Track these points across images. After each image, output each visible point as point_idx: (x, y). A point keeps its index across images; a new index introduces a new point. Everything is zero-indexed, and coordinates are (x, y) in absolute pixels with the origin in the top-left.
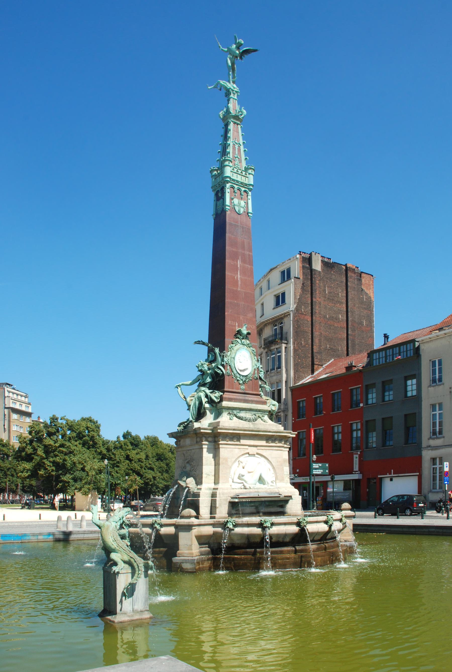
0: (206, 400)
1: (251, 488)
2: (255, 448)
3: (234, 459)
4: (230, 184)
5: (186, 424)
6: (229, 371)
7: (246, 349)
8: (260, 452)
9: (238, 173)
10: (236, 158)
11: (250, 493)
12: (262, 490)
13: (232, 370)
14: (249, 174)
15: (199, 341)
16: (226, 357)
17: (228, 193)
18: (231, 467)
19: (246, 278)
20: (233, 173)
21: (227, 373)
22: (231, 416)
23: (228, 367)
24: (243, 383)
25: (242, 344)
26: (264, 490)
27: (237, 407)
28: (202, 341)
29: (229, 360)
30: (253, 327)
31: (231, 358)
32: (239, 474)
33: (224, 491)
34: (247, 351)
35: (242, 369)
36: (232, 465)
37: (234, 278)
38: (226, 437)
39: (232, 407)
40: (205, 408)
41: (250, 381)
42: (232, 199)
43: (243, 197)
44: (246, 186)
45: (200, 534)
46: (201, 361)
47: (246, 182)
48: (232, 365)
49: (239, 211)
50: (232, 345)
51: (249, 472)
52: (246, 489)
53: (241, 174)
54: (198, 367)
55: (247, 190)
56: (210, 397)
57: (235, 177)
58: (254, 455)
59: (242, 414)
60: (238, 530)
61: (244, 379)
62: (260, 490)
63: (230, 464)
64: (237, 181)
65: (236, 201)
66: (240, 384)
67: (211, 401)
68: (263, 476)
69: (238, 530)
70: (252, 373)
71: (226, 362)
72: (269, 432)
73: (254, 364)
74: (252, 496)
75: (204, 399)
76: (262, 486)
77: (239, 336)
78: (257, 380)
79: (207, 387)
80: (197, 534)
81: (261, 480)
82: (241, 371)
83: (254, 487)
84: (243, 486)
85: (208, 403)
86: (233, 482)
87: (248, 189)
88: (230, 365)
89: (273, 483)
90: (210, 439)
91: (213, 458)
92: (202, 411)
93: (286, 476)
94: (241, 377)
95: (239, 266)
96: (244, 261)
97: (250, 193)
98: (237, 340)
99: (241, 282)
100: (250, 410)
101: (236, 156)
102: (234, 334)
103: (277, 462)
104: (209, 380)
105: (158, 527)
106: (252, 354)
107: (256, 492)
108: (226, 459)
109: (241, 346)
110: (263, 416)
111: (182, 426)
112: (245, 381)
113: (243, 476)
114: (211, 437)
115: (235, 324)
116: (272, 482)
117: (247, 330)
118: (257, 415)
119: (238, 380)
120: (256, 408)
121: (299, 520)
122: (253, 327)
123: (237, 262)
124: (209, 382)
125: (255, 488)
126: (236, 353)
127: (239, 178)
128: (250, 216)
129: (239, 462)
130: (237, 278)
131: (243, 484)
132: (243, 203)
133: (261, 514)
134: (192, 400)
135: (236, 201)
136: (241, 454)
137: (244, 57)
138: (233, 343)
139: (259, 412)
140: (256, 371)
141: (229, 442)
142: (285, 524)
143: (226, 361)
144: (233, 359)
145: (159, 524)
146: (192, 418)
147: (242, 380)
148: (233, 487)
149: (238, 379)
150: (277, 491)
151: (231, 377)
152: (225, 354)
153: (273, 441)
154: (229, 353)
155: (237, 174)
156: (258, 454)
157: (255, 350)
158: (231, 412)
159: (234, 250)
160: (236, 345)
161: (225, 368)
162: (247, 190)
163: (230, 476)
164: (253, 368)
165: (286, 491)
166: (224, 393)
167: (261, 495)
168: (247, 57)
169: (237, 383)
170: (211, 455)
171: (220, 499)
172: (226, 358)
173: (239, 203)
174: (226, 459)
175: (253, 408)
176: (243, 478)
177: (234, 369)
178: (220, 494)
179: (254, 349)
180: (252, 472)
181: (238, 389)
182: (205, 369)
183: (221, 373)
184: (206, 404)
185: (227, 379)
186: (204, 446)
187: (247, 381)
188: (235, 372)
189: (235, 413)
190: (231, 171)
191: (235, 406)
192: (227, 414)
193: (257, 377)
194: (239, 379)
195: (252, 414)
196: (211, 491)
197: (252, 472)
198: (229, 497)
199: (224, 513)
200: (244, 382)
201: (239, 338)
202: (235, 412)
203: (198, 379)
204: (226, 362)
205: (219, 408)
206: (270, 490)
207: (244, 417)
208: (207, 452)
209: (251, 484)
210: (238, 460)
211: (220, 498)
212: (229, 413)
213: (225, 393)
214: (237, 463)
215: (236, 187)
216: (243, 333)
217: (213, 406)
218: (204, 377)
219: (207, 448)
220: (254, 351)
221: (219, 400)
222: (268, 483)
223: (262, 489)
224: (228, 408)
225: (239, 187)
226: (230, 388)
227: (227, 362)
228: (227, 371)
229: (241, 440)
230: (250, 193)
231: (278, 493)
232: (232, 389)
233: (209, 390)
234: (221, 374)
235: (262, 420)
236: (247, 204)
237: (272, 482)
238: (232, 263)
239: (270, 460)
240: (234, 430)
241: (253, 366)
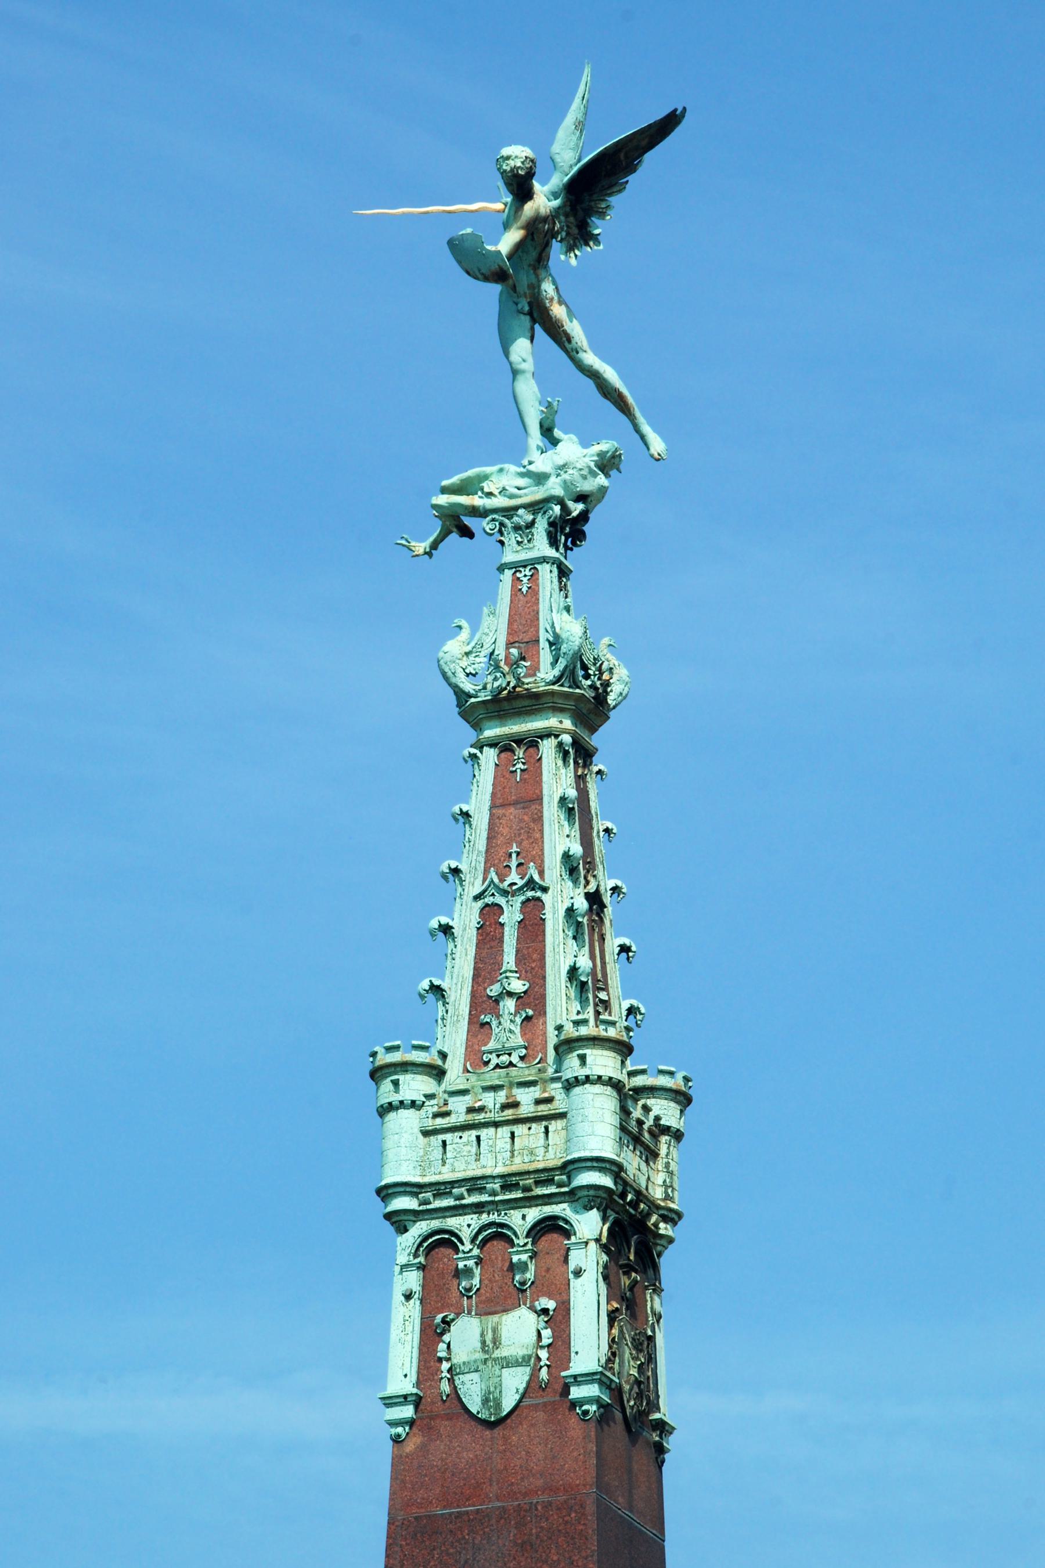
9: (480, 1117)
17: (408, 1297)
20: (448, 1137)
43: (530, 1275)
44: (550, 1181)
49: (485, 1401)
53: (509, 1113)
64: (474, 1184)
128: (581, 1402)
155: (474, 1133)
173: (490, 1343)
190: (426, 1133)
215: (465, 1225)
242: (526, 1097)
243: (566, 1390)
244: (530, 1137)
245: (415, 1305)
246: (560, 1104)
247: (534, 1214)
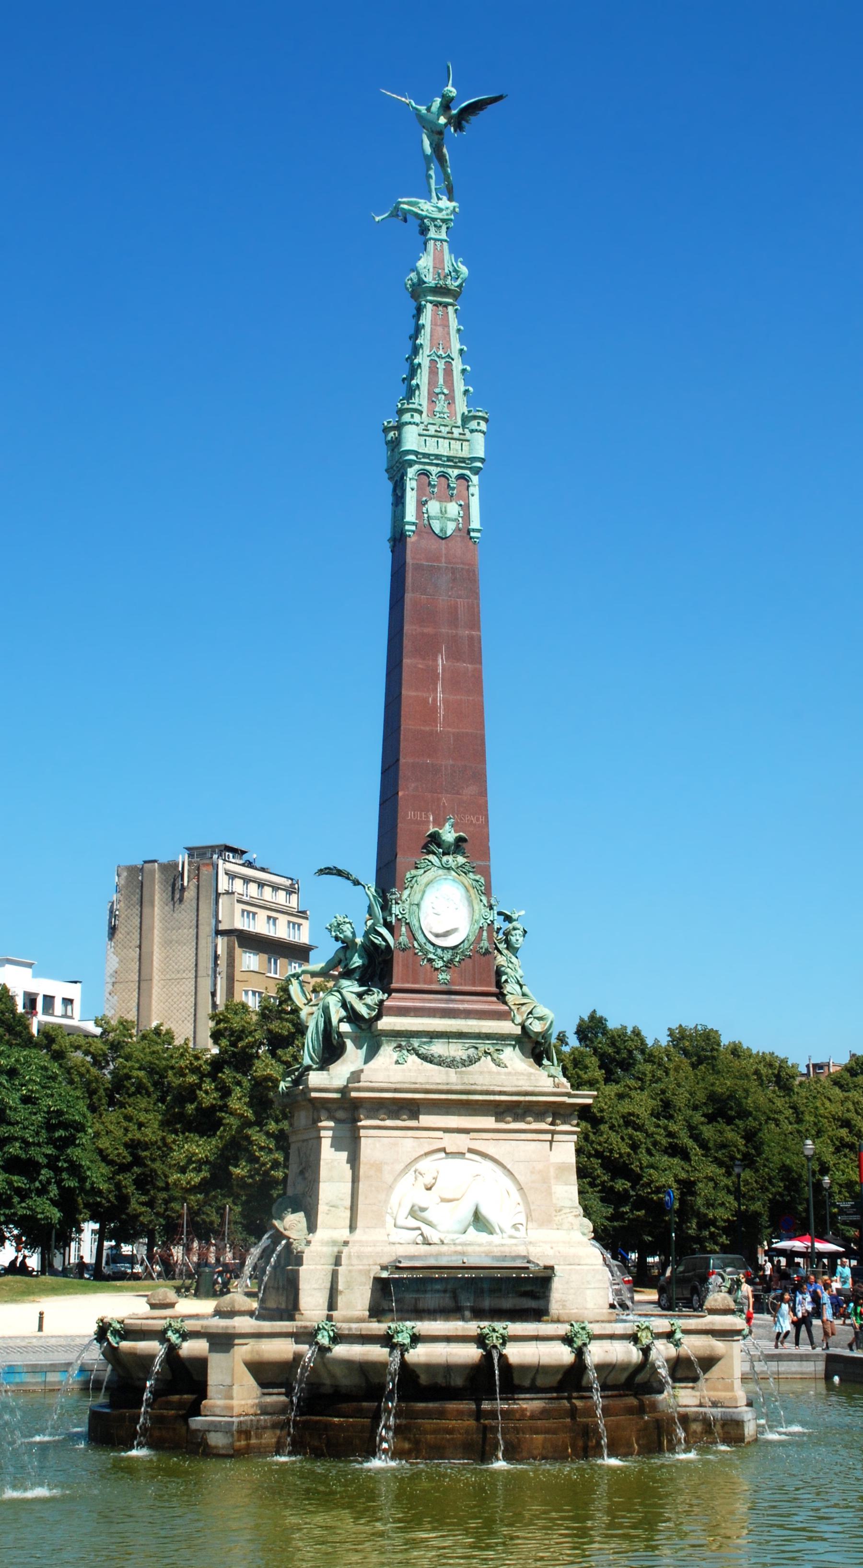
0: (343, 1013)
1: (445, 1242)
2: (463, 1136)
3: (401, 1166)
4: (417, 467)
5: (296, 1073)
6: (404, 939)
7: (454, 880)
8: (476, 1145)
9: (439, 434)
10: (438, 394)
11: (438, 1255)
12: (477, 1249)
13: (413, 935)
14: (472, 431)
15: (329, 868)
16: (397, 903)
17: (413, 489)
18: (391, 1187)
19: (459, 697)
20: (427, 438)
21: (400, 944)
23: (403, 929)
24: (446, 966)
25: (444, 868)
26: (482, 1249)
27: (420, 1029)
29: (406, 911)
30: (478, 820)
31: (411, 904)
32: (413, 1207)
33: (362, 1249)
34: (456, 885)
35: (440, 931)
36: (395, 1180)
37: (426, 700)
38: (378, 1110)
39: (407, 1031)
40: (340, 1035)
41: (467, 960)
42: (421, 504)
43: (455, 492)
44: (464, 462)
45: (256, 1358)
46: (337, 915)
47: (465, 454)
48: (414, 923)
49: (441, 530)
50: (414, 872)
51: (443, 1200)
52: (430, 1244)
53: (450, 436)
54: (330, 931)
55: (467, 472)
56: (352, 1008)
57: (431, 447)
58: (461, 1155)
59: (438, 1048)
60: (341, 1351)
61: (447, 956)
62: (469, 1249)
63: (389, 1178)
64: (438, 457)
65: (433, 507)
66: (436, 969)
67: (353, 1017)
68: (484, 1211)
69: (341, 1351)
70: (472, 938)
71: (396, 916)
72: (501, 1093)
73: (476, 917)
74: (443, 1262)
75: (337, 1012)
76: (483, 1237)
77: (433, 848)
78: (487, 956)
79: (356, 980)
80: (248, 1357)
81: (479, 1220)
82: (437, 936)
83: (453, 1240)
84: (420, 1238)
85: (348, 1022)
86: (395, 1226)
87: (470, 469)
88: (408, 924)
89: (517, 1229)
90: (340, 1114)
91: (347, 1162)
92: (335, 1042)
93: (568, 1210)
94: (439, 951)
95: (440, 671)
96: (454, 655)
97: (475, 479)
98: (431, 857)
99: (444, 709)
100: (460, 1035)
101: (437, 390)
102: (423, 842)
103: (532, 1172)
104: (357, 961)
105: (174, 1338)
106: (472, 891)
107: (456, 1253)
108: (378, 1167)
109: (441, 872)
110: (497, 1050)
111: (289, 1079)
112: (451, 961)
113: (423, 1210)
114: (344, 1109)
115: (428, 817)
116: (514, 1226)
117: (456, 831)
118: (482, 1048)
119: (430, 961)
120: (477, 1031)
122: (478, 820)
123: (436, 660)
124: (358, 967)
125: (457, 1241)
126: (424, 892)
127: (444, 448)
128: (474, 538)
129: (415, 1171)
130: (435, 700)
131: (419, 1232)
132: (453, 509)
133: (467, 1314)
134: (312, 1014)
135: (433, 507)
136: (423, 1153)
138: (417, 868)
139: (488, 1039)
140: (485, 934)
141: (389, 1123)
142: (448, 1339)
143: (398, 913)
144: (415, 907)
145: (176, 1331)
146: (312, 1059)
147: (442, 958)
148: (392, 1239)
149: (431, 956)
150: (524, 1253)
151: (411, 952)
152: (394, 897)
154: (406, 893)
155: (436, 439)
156: (470, 1151)
157: (482, 880)
158: (403, 1044)
159: (426, 630)
160: (425, 872)
161: (396, 930)
162: (467, 472)
163: (389, 1211)
164: (476, 927)
165: (550, 1252)
166: (389, 995)
167: (471, 1261)
169: (429, 966)
170: (344, 1155)
171: (350, 1271)
172: (398, 906)
173: (443, 512)
174: (378, 1167)
175: (465, 1030)
176: (425, 1215)
177: (420, 932)
178: (349, 1257)
179: (477, 877)
180: (458, 1200)
181: (431, 982)
182: (345, 937)
183: (384, 943)
184: (341, 1024)
185: (399, 960)
186: (323, 1133)
187: (457, 959)
188: (422, 940)
189: (416, 1045)
190: (420, 435)
191: (414, 1028)
192: (391, 1048)
193: (487, 950)
194: (434, 957)
195: (467, 1045)
196: (336, 1249)
197: (458, 1200)
198: (375, 1264)
199: (359, 1308)
200: (449, 964)
201: (434, 853)
202: (416, 1043)
203: (336, 960)
204: (396, 916)
205: (376, 1033)
206: (502, 1249)
207: (436, 1055)
208: (332, 1146)
209: (448, 1232)
210: (413, 1169)
211: (350, 1268)
212: (399, 1046)
213: (393, 994)
214: (411, 1175)
215: (434, 470)
216: (444, 841)
217: (360, 1027)
218: (348, 954)
219: (333, 1138)
220: (477, 881)
221: (374, 1013)
222: (502, 1231)
223: (480, 1245)
224: (395, 1034)
225: (442, 469)
226: (408, 982)
227: (400, 917)
228: (401, 939)
229: (421, 1117)
230: (475, 479)
231: (524, 1257)
232: (414, 982)
233: (361, 986)
234: (383, 947)
235: (493, 1060)
236: (466, 508)
237: (514, 1226)
238: (420, 666)
239: (509, 1167)
240: (396, 1090)
241: (473, 922)
242: (456, 432)
243: (469, 532)
244: (456, 445)
245: (415, 492)
246: (468, 435)
247: (456, 472)
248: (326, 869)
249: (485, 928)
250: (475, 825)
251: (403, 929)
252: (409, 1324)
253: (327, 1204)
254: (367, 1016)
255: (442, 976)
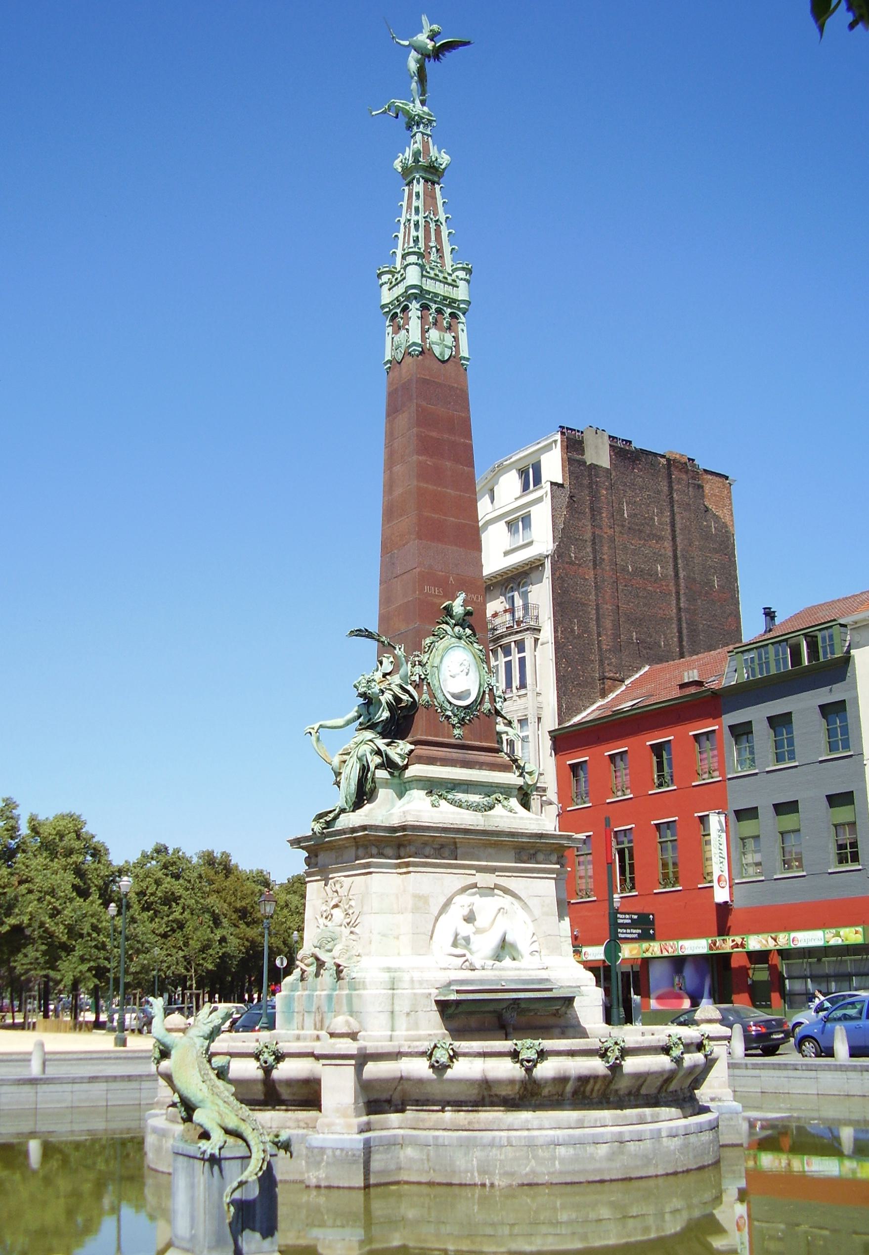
8: (503, 882)
10: (432, 247)
15: (360, 630)
22: (433, 798)
23: (425, 687)
28: (367, 630)
30: (477, 598)
34: (466, 652)
35: (456, 690)
52: (474, 970)
65: (434, 334)
67: (388, 764)
79: (379, 733)
97: (463, 319)
103: (543, 906)
106: (478, 659)
119: (448, 717)
121: (603, 1043)
122: (477, 598)
132: (448, 338)
137: (443, 55)
140: (487, 696)
143: (421, 673)
149: (449, 713)
153: (532, 858)
168: (449, 57)
179: (481, 648)
188: (441, 698)
201: (447, 623)
205: (405, 780)
218: (371, 709)
227: (423, 677)
233: (384, 738)
235: (503, 806)
238: (429, 463)
247: (449, 311)
248: (357, 631)
249: (487, 692)
250: (475, 602)
251: (425, 687)
252: (536, 1042)
253: (379, 933)
254: (401, 764)
255: (456, 732)
